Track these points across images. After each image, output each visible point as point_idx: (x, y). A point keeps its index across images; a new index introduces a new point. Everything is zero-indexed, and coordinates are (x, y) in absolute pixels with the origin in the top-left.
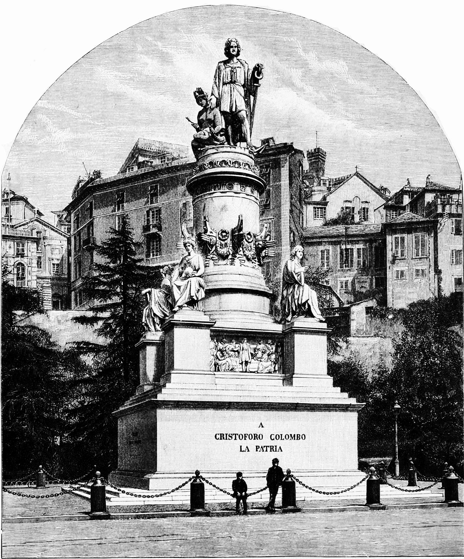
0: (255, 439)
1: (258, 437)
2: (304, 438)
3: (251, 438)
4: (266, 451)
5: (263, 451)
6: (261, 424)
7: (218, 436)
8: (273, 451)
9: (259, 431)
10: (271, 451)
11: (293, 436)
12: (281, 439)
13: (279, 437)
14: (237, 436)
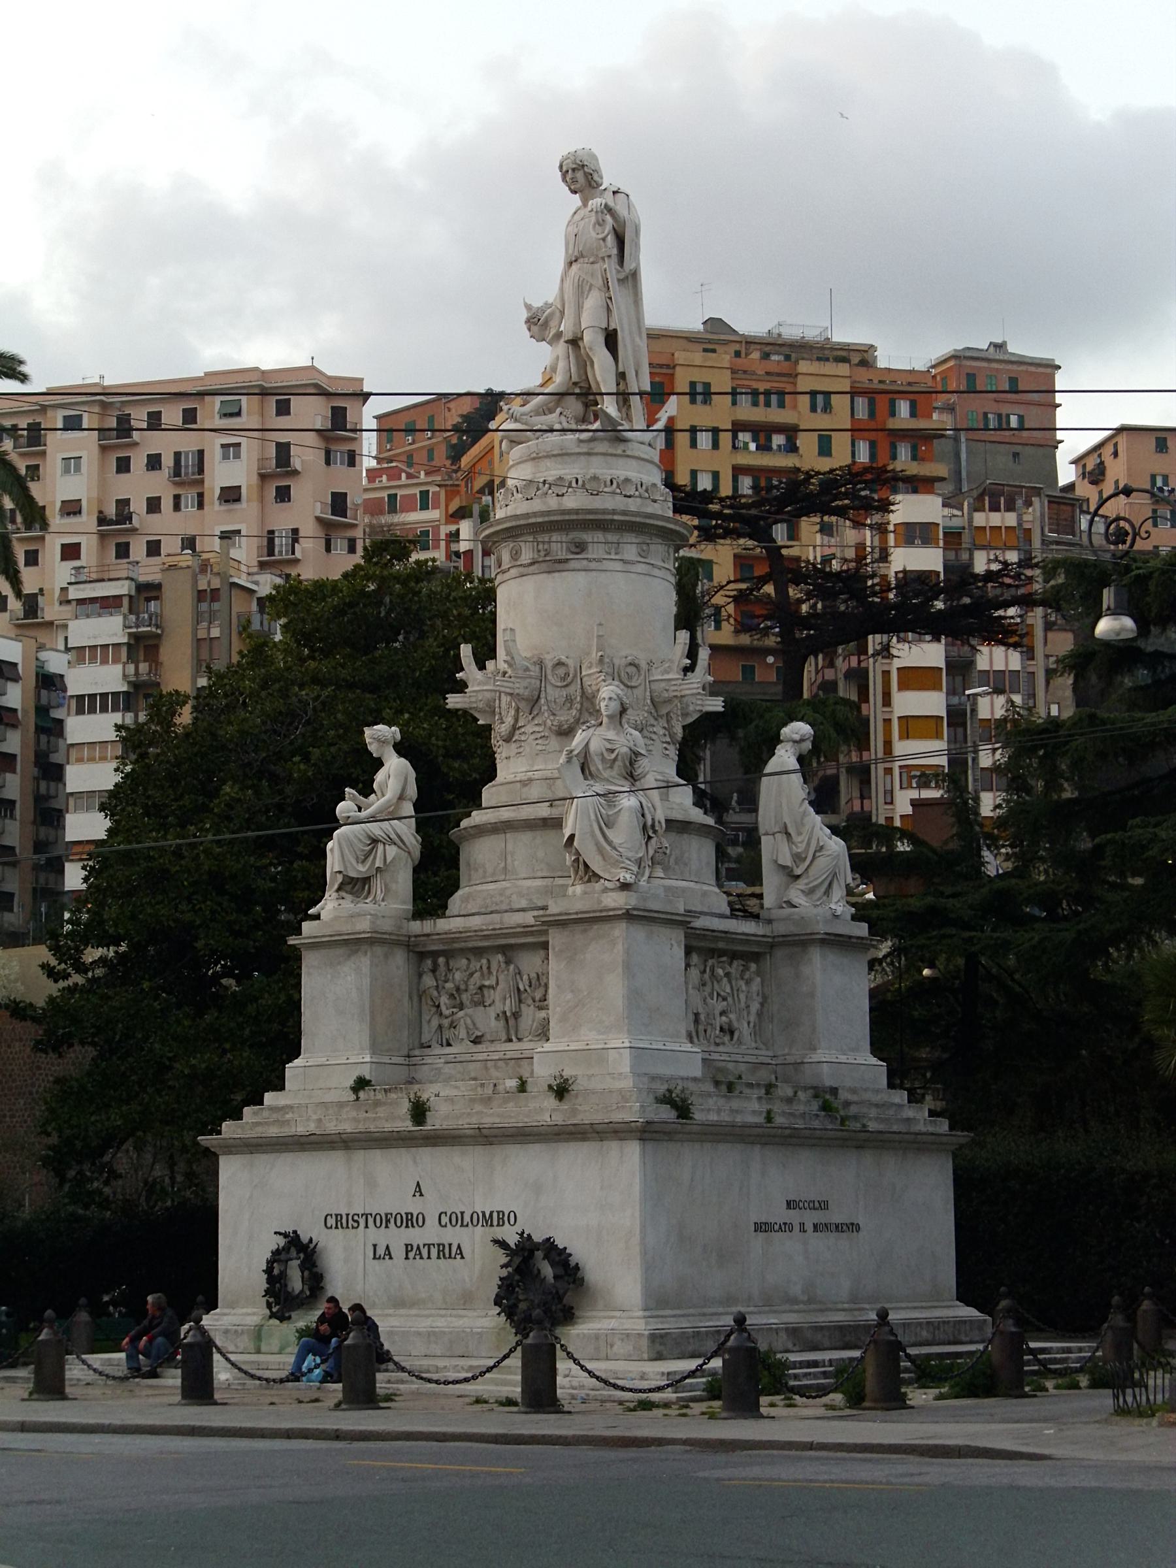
0: (407, 1226)
3: (399, 1224)
4: (429, 1258)
5: (421, 1258)
7: (331, 1221)
9: (413, 1206)
10: (439, 1258)
12: (462, 1225)
13: (457, 1220)
14: (371, 1220)
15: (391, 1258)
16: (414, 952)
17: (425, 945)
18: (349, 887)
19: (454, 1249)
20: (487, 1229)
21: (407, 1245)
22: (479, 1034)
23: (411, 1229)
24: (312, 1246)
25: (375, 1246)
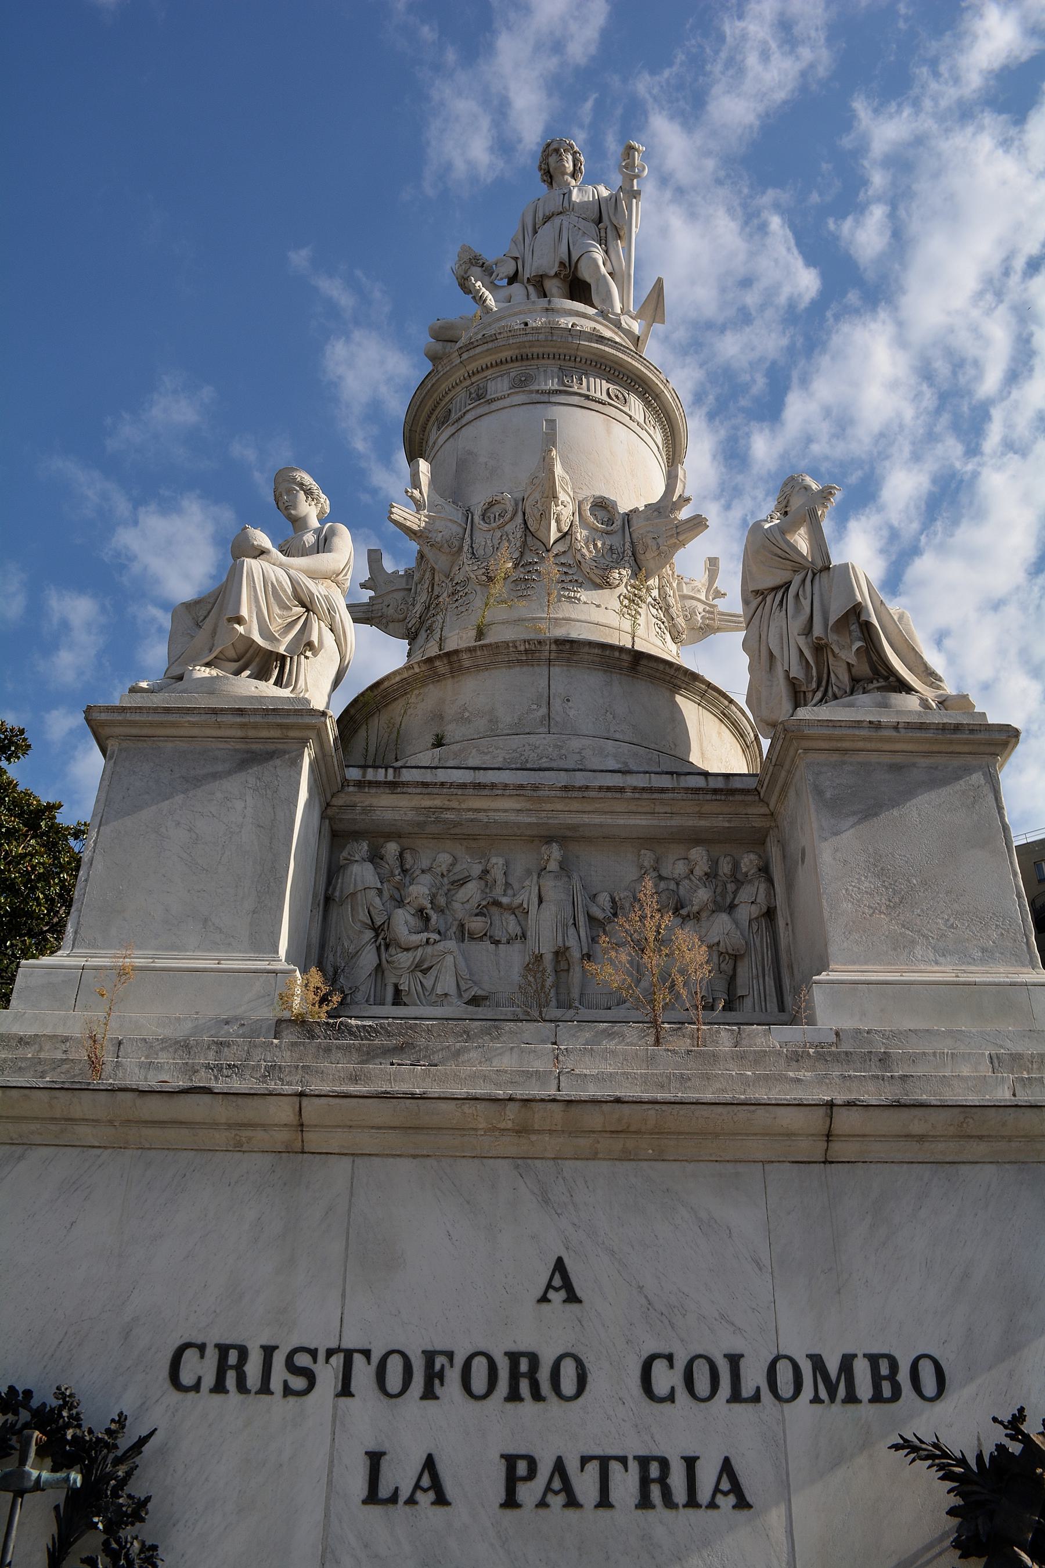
0: (514, 1396)
1: (544, 1375)
2: (929, 1386)
3: (479, 1384)
4: (604, 1502)
5: (572, 1502)
6: (560, 1266)
8: (669, 1502)
10: (645, 1503)
11: (833, 1366)
12: (736, 1397)
14: (363, 1373)
15: (441, 1500)
16: (331, 819)
17: (367, 810)
18: (235, 666)
19: (707, 1476)
20: (837, 1408)
21: (510, 1460)
22: (480, 993)
23: (528, 1407)
24: (124, 1443)
25: (375, 1459)
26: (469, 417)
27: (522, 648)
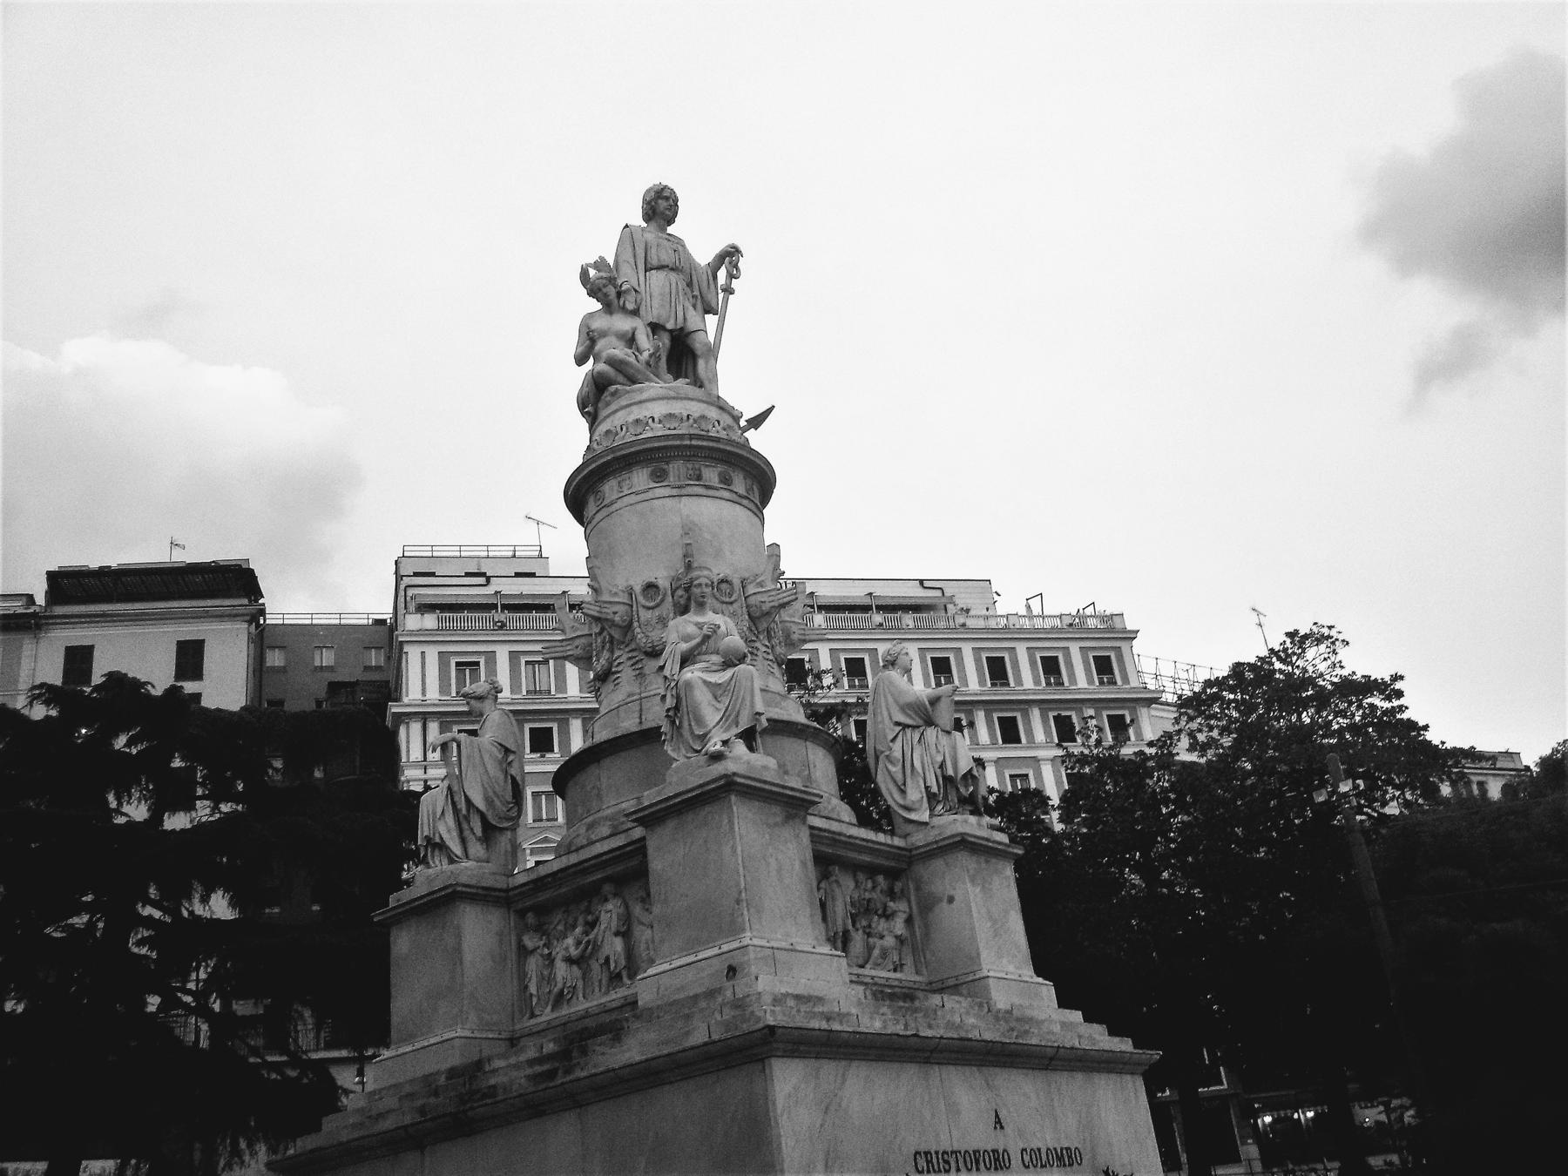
0: (996, 1169)
7: (922, 1163)
12: (1042, 1166)
26: (689, 490)
27: (799, 727)
